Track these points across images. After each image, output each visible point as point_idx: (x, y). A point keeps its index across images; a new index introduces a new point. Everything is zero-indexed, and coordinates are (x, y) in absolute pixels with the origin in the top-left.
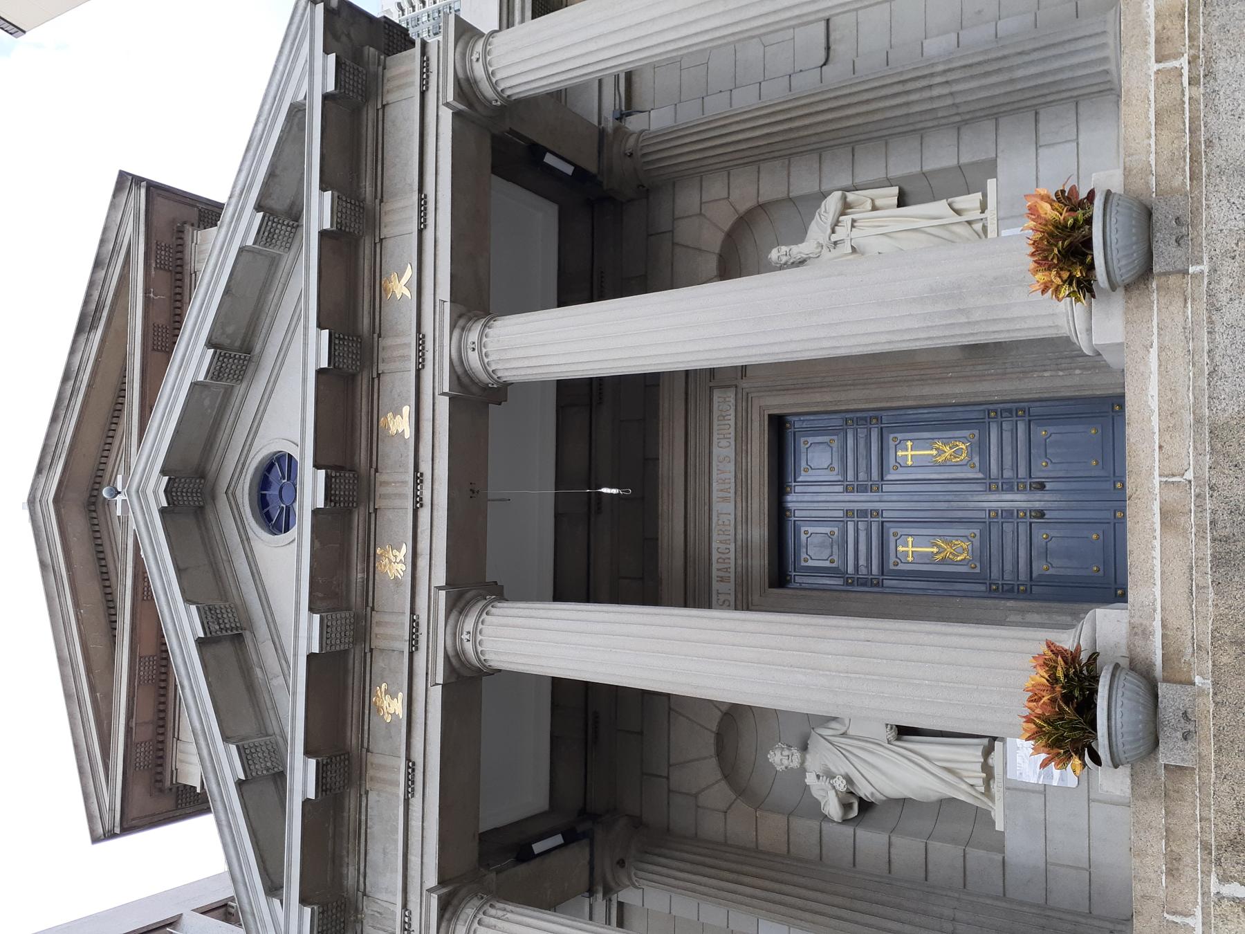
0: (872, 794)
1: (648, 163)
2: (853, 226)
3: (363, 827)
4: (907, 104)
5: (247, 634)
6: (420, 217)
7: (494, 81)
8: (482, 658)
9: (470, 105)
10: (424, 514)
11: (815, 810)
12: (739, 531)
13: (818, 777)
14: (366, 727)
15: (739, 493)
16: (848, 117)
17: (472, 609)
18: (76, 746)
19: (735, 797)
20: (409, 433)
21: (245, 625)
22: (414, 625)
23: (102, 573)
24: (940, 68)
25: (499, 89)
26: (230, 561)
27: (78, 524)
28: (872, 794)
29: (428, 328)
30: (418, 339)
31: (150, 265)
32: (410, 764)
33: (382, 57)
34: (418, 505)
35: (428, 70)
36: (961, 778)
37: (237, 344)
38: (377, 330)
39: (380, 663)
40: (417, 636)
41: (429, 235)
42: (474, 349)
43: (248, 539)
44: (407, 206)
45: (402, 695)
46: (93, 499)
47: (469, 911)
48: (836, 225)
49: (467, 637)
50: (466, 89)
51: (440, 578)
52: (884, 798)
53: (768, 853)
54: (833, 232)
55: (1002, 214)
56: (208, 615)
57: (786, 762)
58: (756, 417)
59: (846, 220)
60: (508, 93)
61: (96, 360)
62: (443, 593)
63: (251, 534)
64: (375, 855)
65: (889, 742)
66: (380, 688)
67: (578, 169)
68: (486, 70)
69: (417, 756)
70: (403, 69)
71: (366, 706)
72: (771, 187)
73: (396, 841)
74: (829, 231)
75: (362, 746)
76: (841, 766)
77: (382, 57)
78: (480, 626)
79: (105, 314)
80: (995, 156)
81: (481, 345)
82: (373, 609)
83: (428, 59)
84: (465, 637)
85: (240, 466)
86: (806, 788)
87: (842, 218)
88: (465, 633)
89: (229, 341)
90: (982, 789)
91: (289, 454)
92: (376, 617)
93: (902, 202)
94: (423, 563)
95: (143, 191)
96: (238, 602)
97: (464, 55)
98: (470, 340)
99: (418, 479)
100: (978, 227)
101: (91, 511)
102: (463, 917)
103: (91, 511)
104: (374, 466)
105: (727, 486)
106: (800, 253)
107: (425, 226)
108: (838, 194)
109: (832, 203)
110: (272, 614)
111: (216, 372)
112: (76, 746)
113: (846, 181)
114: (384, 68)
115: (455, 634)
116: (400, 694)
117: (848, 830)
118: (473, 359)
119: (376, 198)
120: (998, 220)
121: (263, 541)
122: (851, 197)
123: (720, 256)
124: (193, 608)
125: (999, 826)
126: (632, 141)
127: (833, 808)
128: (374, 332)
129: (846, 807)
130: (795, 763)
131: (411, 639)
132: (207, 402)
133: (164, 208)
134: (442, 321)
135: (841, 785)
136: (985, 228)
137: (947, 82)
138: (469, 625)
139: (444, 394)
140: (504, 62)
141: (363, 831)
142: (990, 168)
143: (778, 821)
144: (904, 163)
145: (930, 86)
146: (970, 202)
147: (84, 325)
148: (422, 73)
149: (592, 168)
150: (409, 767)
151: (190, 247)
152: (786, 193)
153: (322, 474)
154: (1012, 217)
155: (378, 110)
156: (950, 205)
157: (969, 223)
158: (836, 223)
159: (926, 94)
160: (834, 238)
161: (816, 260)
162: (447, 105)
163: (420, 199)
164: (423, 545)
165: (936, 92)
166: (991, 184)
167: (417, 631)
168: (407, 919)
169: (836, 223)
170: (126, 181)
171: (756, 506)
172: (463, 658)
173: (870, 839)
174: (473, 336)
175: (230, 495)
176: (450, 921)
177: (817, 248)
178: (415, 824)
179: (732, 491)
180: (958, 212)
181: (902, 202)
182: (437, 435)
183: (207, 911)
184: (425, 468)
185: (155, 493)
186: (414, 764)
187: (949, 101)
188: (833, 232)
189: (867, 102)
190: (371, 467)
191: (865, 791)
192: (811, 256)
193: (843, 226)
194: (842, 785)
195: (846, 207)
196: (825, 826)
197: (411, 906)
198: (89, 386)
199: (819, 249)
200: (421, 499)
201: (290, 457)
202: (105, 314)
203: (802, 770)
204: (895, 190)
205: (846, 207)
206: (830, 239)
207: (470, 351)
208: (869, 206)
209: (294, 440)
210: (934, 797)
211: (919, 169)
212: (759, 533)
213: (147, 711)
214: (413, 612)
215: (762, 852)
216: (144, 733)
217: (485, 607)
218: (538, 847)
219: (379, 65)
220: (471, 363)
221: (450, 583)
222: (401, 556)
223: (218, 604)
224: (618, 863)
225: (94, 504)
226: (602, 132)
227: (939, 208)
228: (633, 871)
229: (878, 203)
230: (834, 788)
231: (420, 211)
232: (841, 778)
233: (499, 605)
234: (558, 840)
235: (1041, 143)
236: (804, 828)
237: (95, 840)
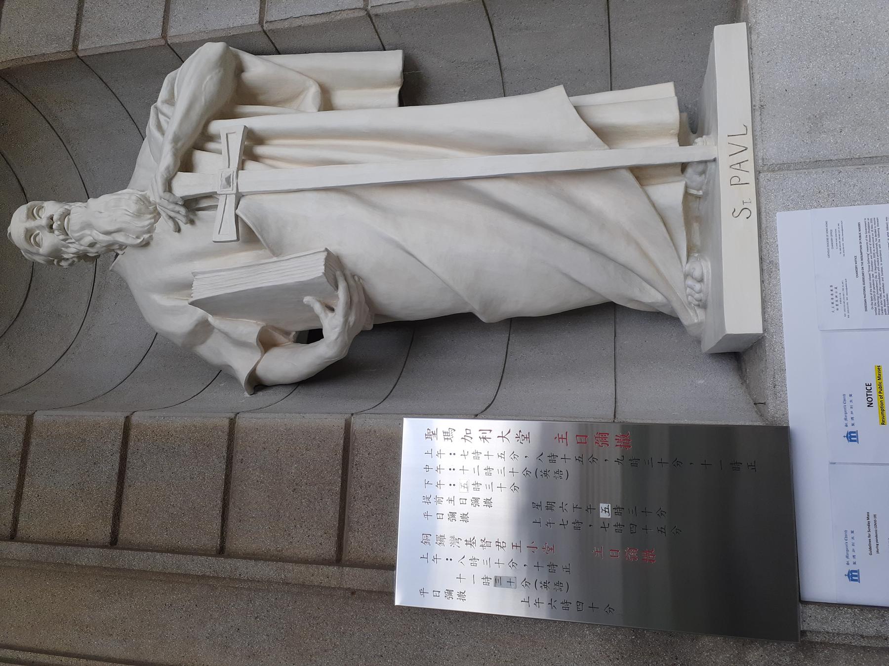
55: (772, 152)
87: (218, 126)
106: (88, 226)
108: (212, 50)
120: (757, 173)
152: (70, 39)
154: (816, 164)
161: (141, 255)
177: (139, 215)
188: (186, 165)
192: (120, 238)
193: (219, 152)
199: (146, 221)
206: (168, 186)
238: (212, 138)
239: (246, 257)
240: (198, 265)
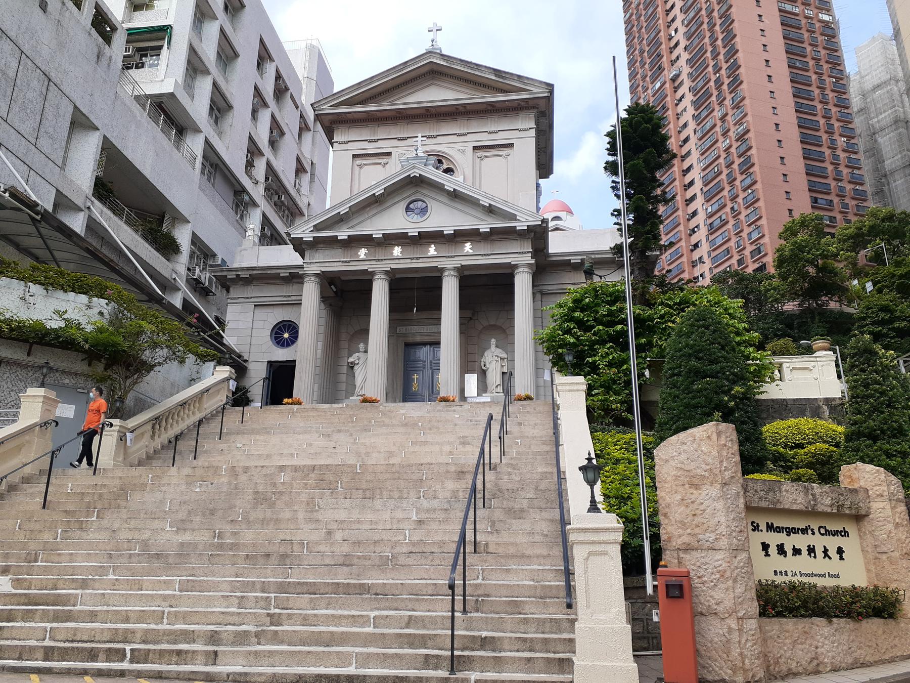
10: (409, 261)
11: (350, 355)
18: (342, 91)
20: (430, 254)
22: (382, 260)
29: (456, 258)
38: (457, 243)
39: (372, 250)
41: (480, 257)
50: (516, 266)
64: (327, 252)
69: (351, 263)
76: (361, 362)
79: (501, 80)
93: (503, 373)
94: (397, 261)
95: (546, 95)
99: (418, 258)
109: (504, 355)
112: (342, 91)
121: (403, 205)
127: (351, 360)
129: (352, 363)
133: (542, 104)
143: (347, 347)
146: (500, 389)
147: (497, 72)
151: (528, 112)
164: (402, 261)
170: (550, 88)
173: (344, 369)
178: (335, 264)
180: (497, 386)
181: (503, 373)
183: (277, 71)
184: (421, 260)
191: (356, 367)
202: (501, 80)
203: (359, 352)
212: (418, 339)
218: (332, 287)
234: (335, 290)
236: (345, 353)
237: (312, 105)
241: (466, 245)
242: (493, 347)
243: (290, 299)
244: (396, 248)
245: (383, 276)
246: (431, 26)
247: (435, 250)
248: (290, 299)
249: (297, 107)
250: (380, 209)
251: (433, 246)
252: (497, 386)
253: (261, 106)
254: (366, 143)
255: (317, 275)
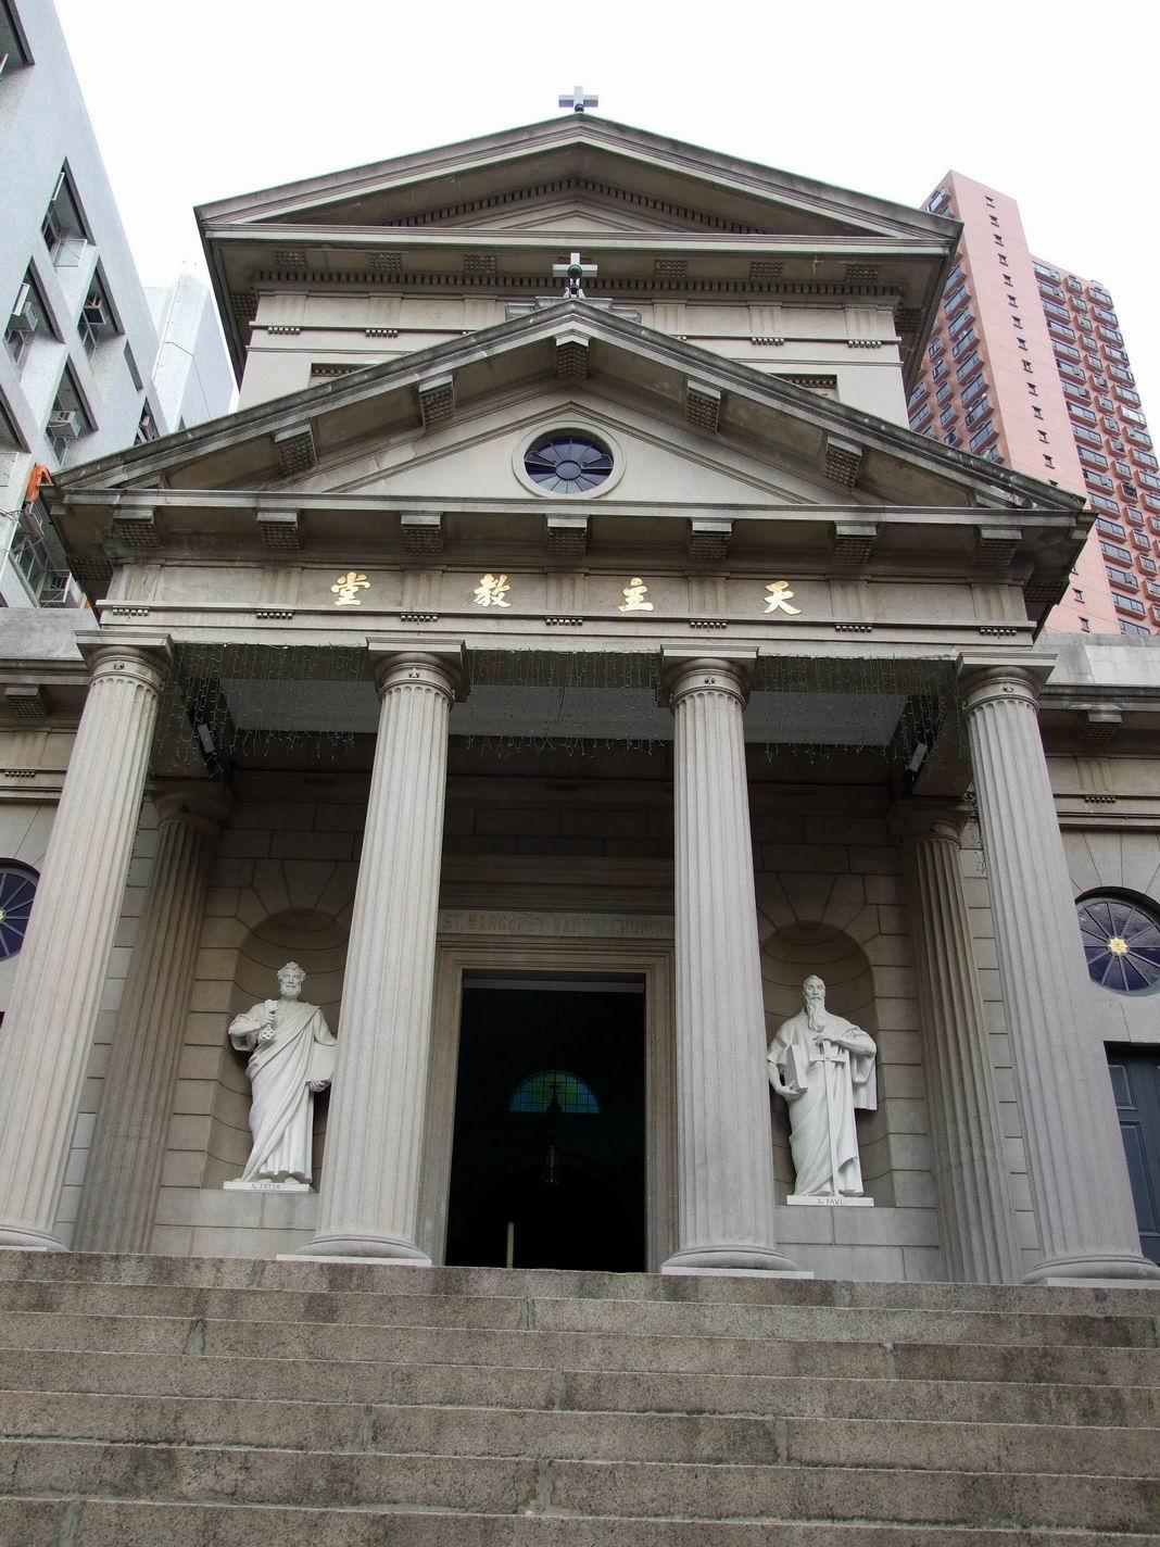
0: (256, 1065)
1: (923, 849)
2: (837, 1063)
3: (228, 564)
4: (955, 1121)
5: (422, 431)
6: (848, 625)
7: (983, 706)
8: (393, 689)
9: (962, 679)
10: (539, 627)
11: (241, 1006)
12: (522, 941)
13: (273, 1013)
14: (326, 566)
15: (563, 941)
16: (948, 1060)
17: (442, 679)
19: (251, 926)
20: (624, 611)
21: (430, 428)
23: (497, 198)
24: (988, 1154)
25: (983, 706)
26: (498, 409)
27: (552, 170)
28: (256, 1065)
29: (732, 631)
30: (721, 621)
31: (850, 259)
32: (290, 615)
33: (1022, 583)
34: (549, 621)
35: (1001, 634)
36: (273, 1151)
37: (728, 418)
38: (735, 576)
39: (389, 581)
40: (416, 620)
41: (830, 634)
42: (707, 682)
43: (522, 427)
44: (860, 610)
45: (357, 604)
46: (582, 184)
47: (149, 676)
48: (840, 1046)
49: (414, 675)
51: (473, 644)
52: (252, 1076)
53: (196, 960)
54: (833, 1043)
55: (835, 1210)
56: (443, 393)
57: (286, 980)
58: (643, 961)
59: (845, 1057)
60: (978, 714)
61: (744, 193)
62: (457, 649)
63: (526, 430)
65: (307, 1084)
66: (365, 581)
67: (917, 775)
68: (993, 699)
69: (298, 622)
70: (1007, 606)
71: (344, 565)
72: (887, 981)
73: (215, 600)
74: (834, 1040)
75: (307, 562)
77: (1022, 583)
78: (425, 687)
80: (898, 1205)
81: (711, 690)
82: (444, 571)
83: (1013, 634)
84: (414, 672)
85: (599, 418)
86: (263, 1000)
87: (847, 1052)
88: (418, 671)
89: (731, 411)
90: (263, 1171)
91: (611, 470)
92: (436, 576)
94: (490, 625)
96: (455, 419)
97: (1011, 675)
98: (717, 678)
100: (827, 1187)
101: (569, 182)
102: (145, 669)
103: (569, 182)
104: (591, 572)
105: (571, 929)
107: (838, 630)
109: (865, 1042)
110: (441, 456)
111: (695, 399)
113: (884, 1059)
114: (1010, 585)
115: (417, 661)
116: (357, 602)
117: (221, 1041)
118: (698, 681)
119: (872, 576)
122: (870, 1063)
123: (820, 924)
124: (450, 379)
125: (228, 1185)
126: (949, 831)
127: (242, 1025)
128: (731, 572)
129: (244, 1039)
130: (285, 989)
131: (413, 614)
132: (666, 385)
134: (737, 649)
135: (265, 1035)
136: (826, 1194)
137: (973, 1160)
138: (426, 676)
139: (662, 649)
140: (1000, 717)
141: (223, 564)
142: (885, 1200)
144: (899, 1117)
145: (970, 1143)
146: (854, 1180)
148: (999, 628)
149: (919, 789)
150: (287, 613)
153: (583, 524)
155: (966, 578)
156: (851, 1160)
157: (831, 1179)
158: (841, 1047)
159: (963, 1139)
160: (827, 1045)
161: (806, 1025)
162: (961, 657)
163: (866, 625)
165: (964, 1148)
166: (869, 1201)
167: (421, 620)
168: (140, 611)
169: (841, 1047)
171: (547, 958)
172: (394, 668)
174: (720, 682)
175: (569, 406)
176: (140, 657)
178: (233, 620)
179: (566, 934)
180: (843, 1169)
181: (861, 1115)
182: (620, 640)
184: (588, 628)
185: (572, 332)
186: (290, 618)
187: (953, 1161)
188: (833, 1043)
189: (962, 1080)
190: (591, 569)
191: (259, 1058)
194: (265, 1036)
195: (857, 1057)
196: (224, 1018)
197: (153, 615)
198: (713, 185)
200: (554, 623)
201: (607, 472)
203: (278, 996)
204: (873, 1106)
205: (857, 1057)
207: (703, 678)
208: (858, 1079)
209: (624, 480)
210: (254, 1125)
211: (891, 1131)
213: (338, 261)
214: (441, 615)
215: (197, 953)
216: (315, 260)
217: (444, 691)
219: (1014, 579)
220: (691, 679)
221: (467, 653)
222: (498, 601)
223: (454, 399)
224: (185, 806)
225: (577, 184)
226: (958, 800)
227: (850, 1149)
228: (176, 821)
229: (862, 1091)
230: (262, 1028)
231: (854, 625)
232: (272, 1035)
233: (446, 705)
235: (906, 1250)
238: (843, 1052)
239: (806, 1063)
240: (803, 1047)
241: (772, 587)
242: (818, 1007)
243: (28, 782)
244: (488, 581)
245: (426, 676)
246: (569, 92)
247: (647, 597)
248: (28, 782)
249: (139, 387)
250: (426, 448)
251: (636, 581)
252: (843, 1169)
253: (43, 335)
254: (360, 337)
255: (150, 655)
